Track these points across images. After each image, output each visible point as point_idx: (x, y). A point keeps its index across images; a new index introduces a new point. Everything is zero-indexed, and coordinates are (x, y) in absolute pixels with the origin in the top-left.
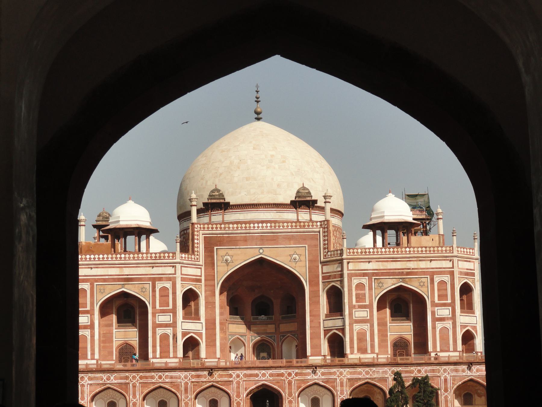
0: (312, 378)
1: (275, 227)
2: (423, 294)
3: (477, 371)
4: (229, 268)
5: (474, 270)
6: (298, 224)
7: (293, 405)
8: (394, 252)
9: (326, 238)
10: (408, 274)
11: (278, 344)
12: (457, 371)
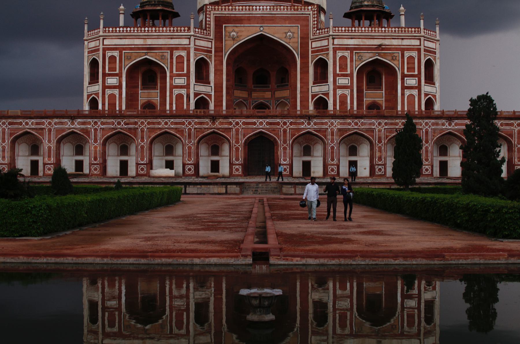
0: (306, 126)
1: (273, 9)
2: (395, 67)
3: (456, 124)
4: (235, 42)
5: (435, 49)
6: (293, 7)
7: (288, 151)
8: (372, 31)
9: (316, 19)
10: (383, 49)
11: (273, 108)
12: (437, 124)
